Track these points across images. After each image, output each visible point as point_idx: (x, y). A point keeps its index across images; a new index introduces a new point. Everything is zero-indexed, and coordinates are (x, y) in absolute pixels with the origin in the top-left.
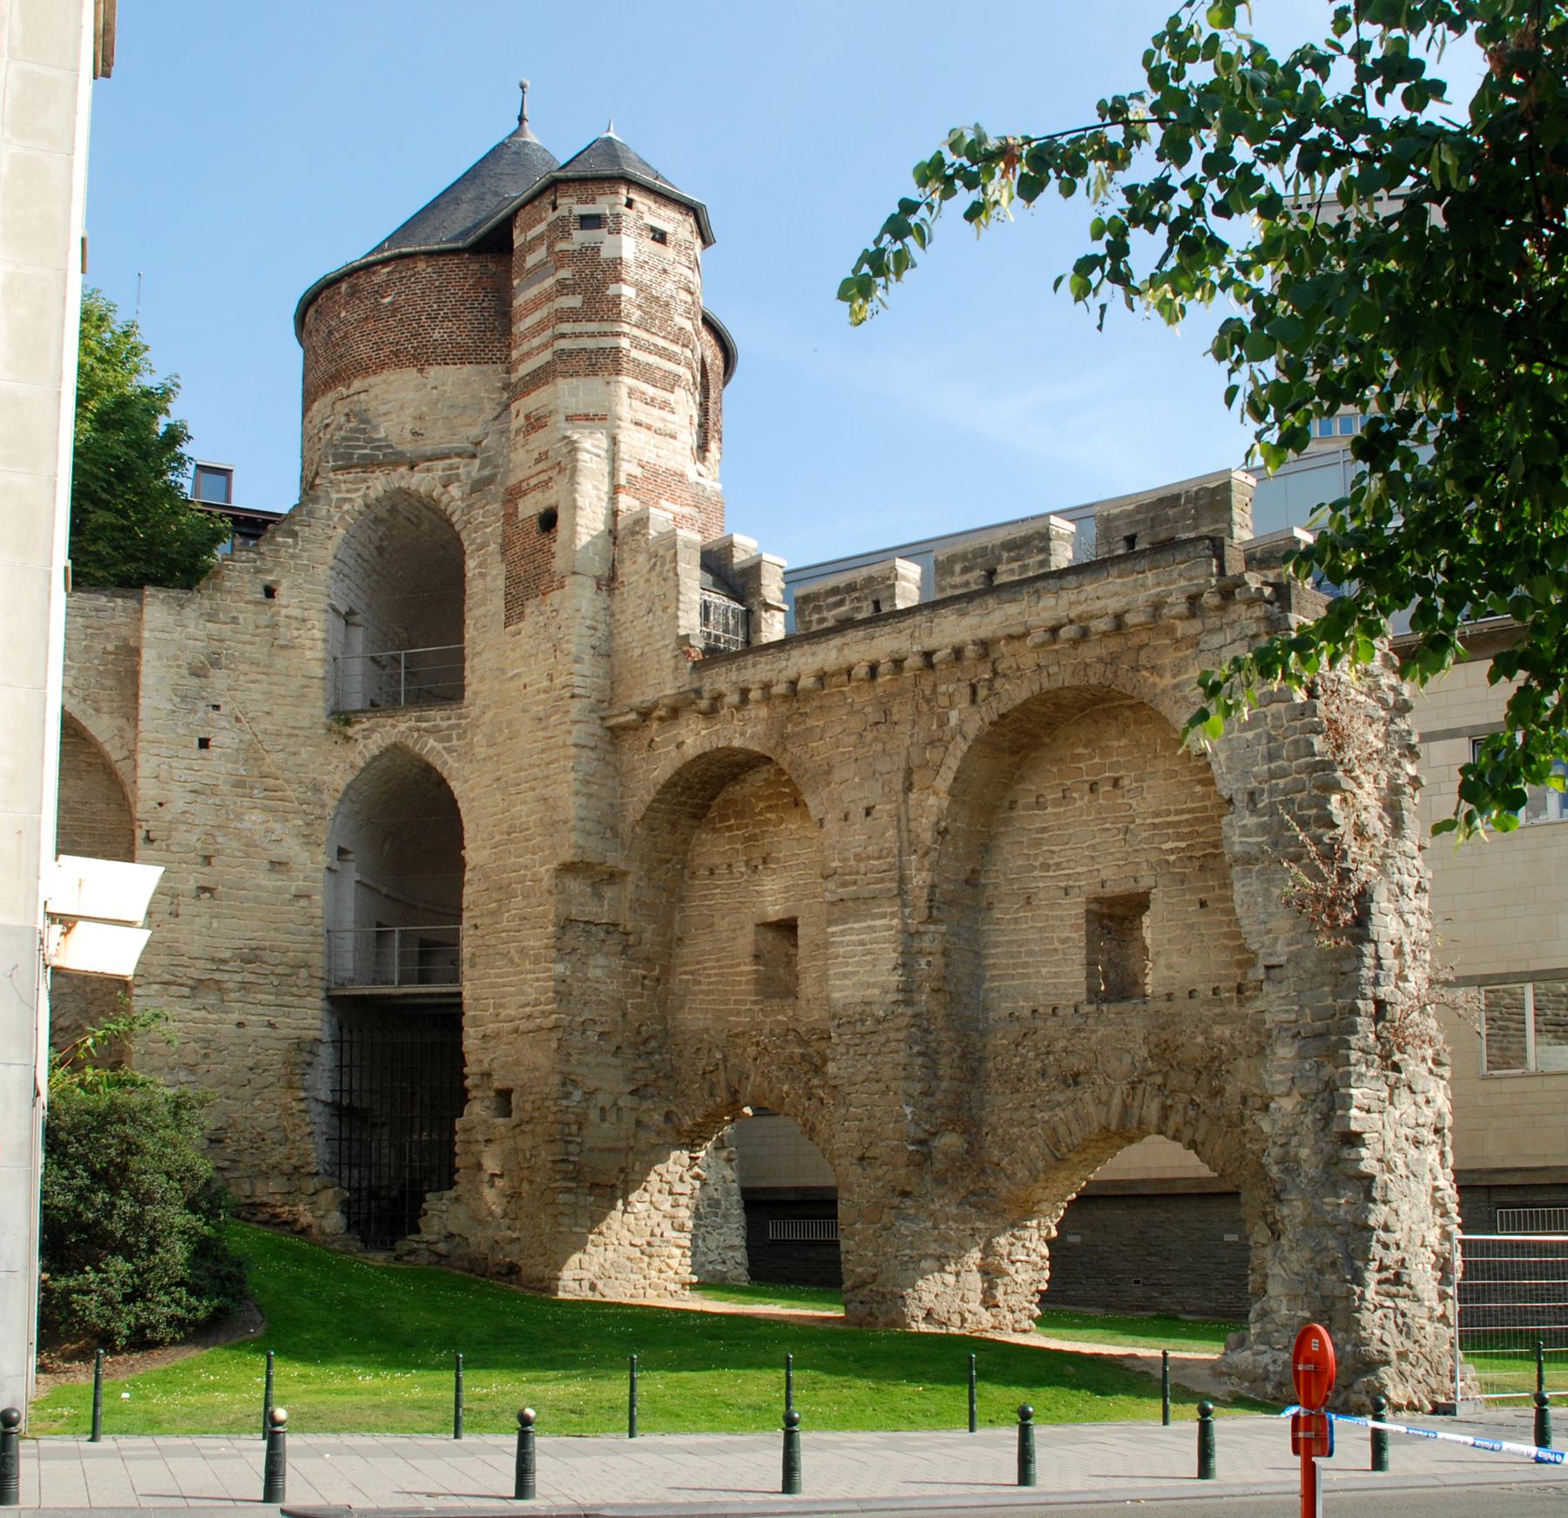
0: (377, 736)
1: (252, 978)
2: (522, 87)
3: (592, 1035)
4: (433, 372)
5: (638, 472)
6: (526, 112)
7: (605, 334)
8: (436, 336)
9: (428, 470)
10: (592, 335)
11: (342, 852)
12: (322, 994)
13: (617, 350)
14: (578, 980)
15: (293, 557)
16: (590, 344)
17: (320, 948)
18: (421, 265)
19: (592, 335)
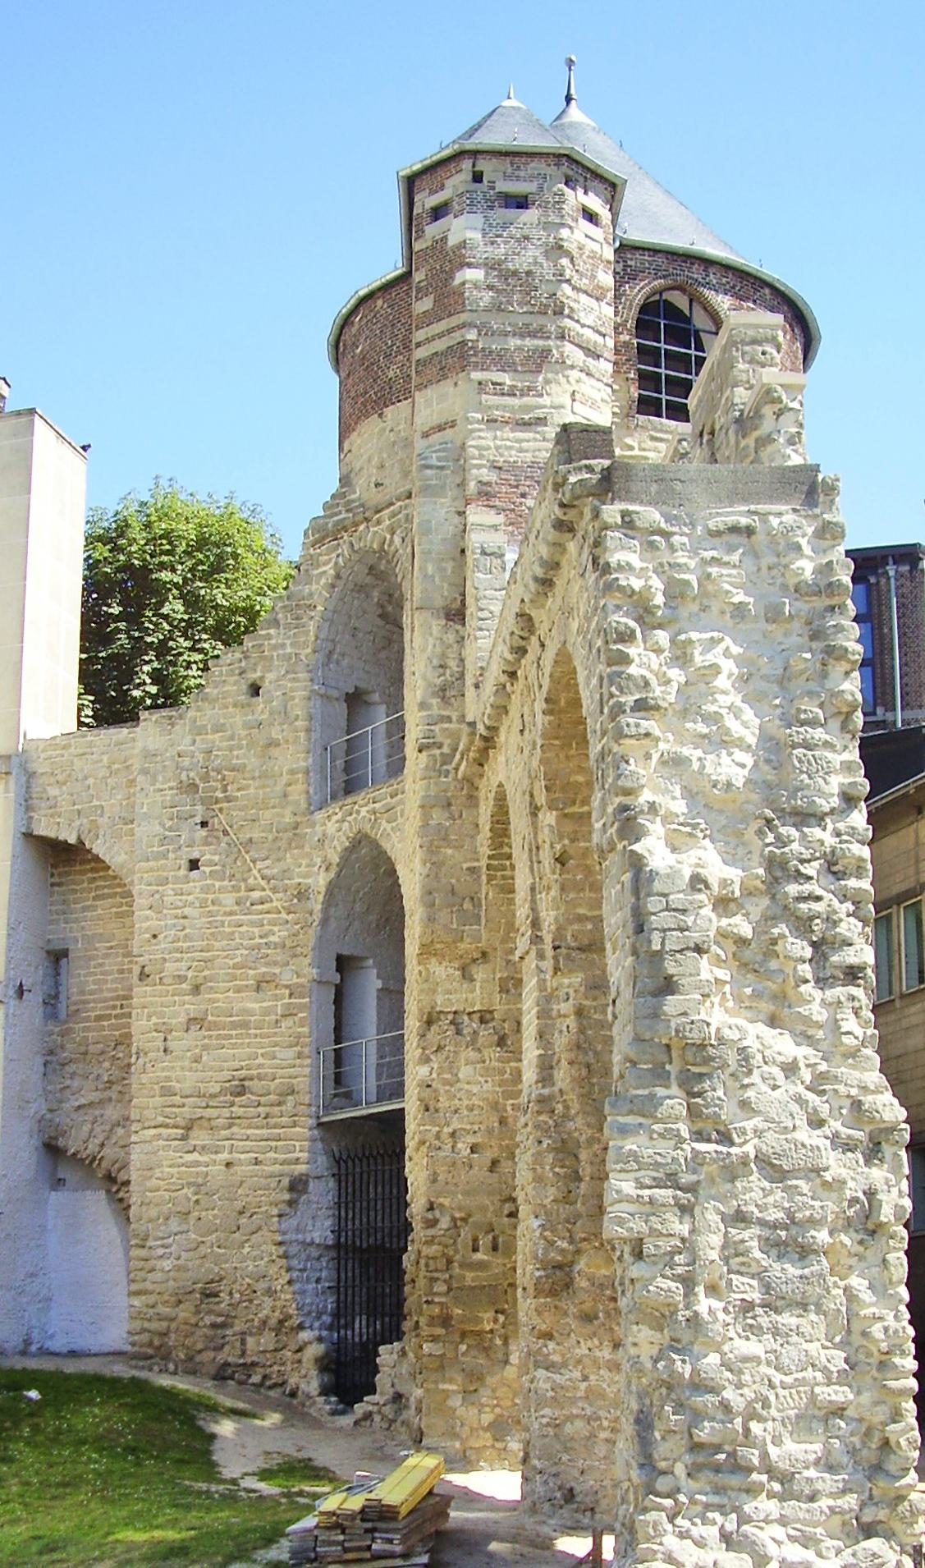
0: (335, 827)
1: (239, 1111)
2: (570, 63)
3: (463, 1147)
4: (389, 411)
5: (493, 477)
6: (573, 91)
7: (450, 331)
8: (391, 374)
9: (379, 522)
10: (441, 335)
11: (343, 964)
12: (312, 1122)
13: (463, 343)
14: (446, 1082)
15: (275, 647)
16: (440, 345)
17: (307, 1071)
18: (380, 302)
19: (441, 335)
